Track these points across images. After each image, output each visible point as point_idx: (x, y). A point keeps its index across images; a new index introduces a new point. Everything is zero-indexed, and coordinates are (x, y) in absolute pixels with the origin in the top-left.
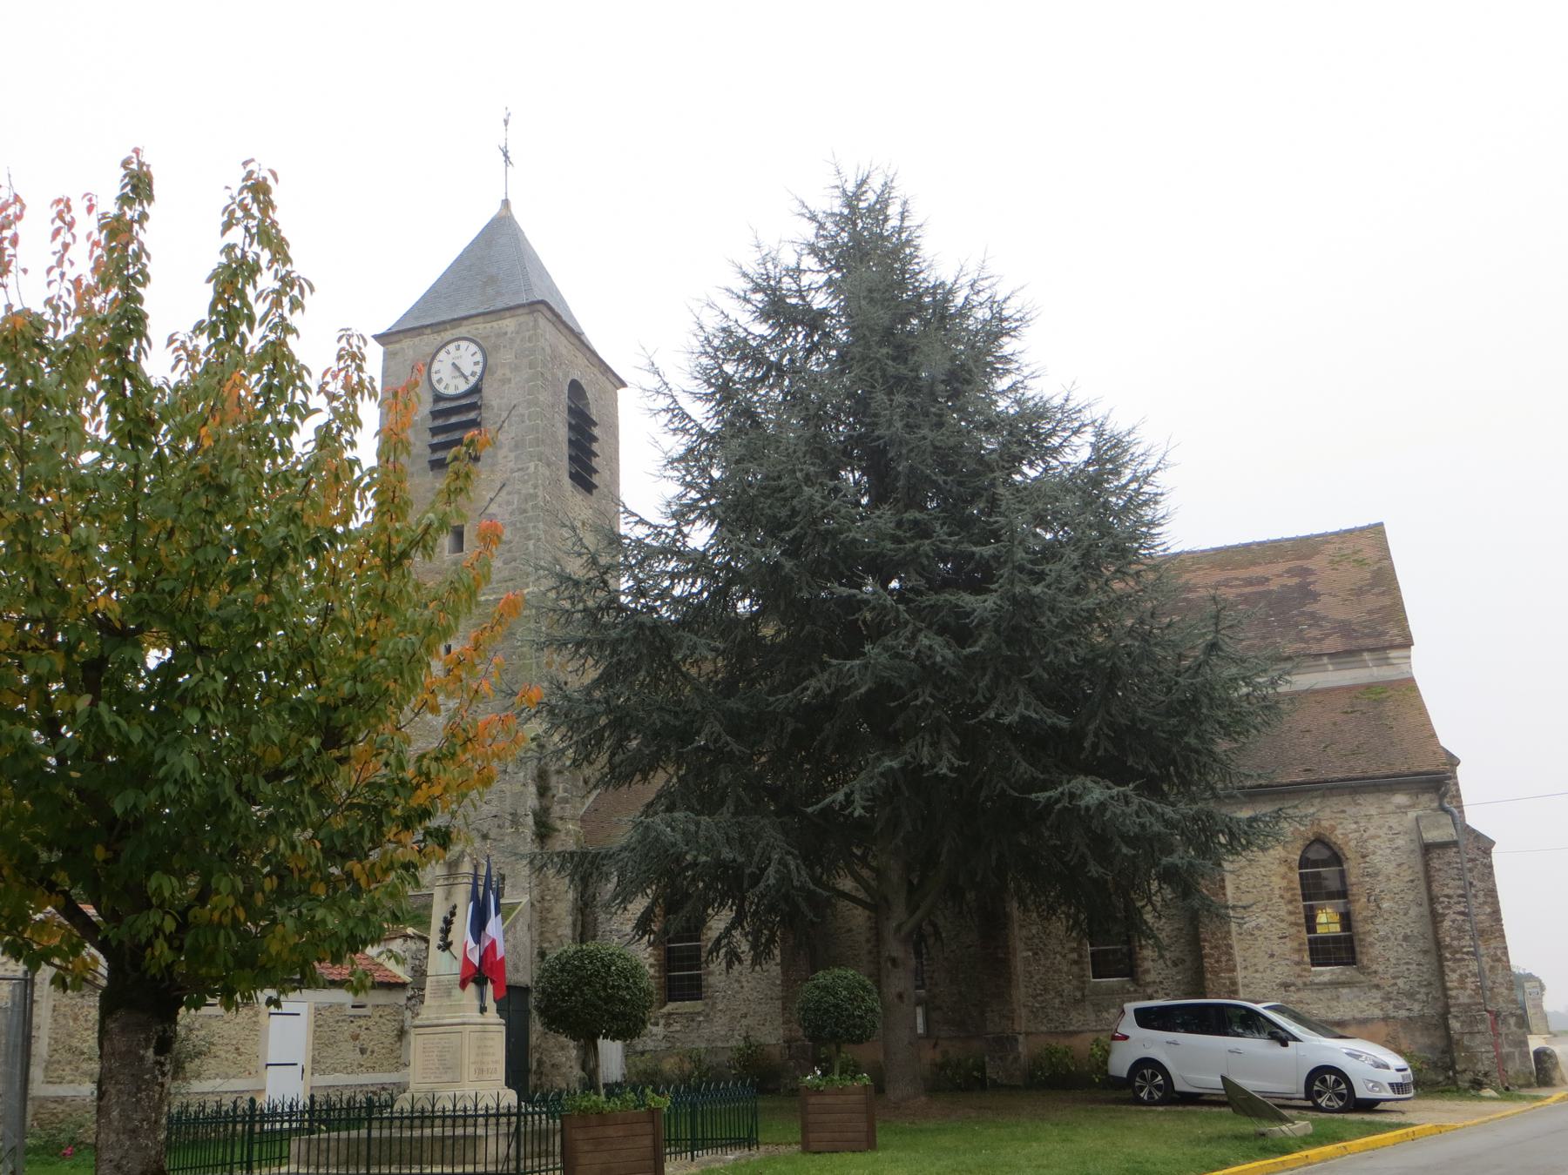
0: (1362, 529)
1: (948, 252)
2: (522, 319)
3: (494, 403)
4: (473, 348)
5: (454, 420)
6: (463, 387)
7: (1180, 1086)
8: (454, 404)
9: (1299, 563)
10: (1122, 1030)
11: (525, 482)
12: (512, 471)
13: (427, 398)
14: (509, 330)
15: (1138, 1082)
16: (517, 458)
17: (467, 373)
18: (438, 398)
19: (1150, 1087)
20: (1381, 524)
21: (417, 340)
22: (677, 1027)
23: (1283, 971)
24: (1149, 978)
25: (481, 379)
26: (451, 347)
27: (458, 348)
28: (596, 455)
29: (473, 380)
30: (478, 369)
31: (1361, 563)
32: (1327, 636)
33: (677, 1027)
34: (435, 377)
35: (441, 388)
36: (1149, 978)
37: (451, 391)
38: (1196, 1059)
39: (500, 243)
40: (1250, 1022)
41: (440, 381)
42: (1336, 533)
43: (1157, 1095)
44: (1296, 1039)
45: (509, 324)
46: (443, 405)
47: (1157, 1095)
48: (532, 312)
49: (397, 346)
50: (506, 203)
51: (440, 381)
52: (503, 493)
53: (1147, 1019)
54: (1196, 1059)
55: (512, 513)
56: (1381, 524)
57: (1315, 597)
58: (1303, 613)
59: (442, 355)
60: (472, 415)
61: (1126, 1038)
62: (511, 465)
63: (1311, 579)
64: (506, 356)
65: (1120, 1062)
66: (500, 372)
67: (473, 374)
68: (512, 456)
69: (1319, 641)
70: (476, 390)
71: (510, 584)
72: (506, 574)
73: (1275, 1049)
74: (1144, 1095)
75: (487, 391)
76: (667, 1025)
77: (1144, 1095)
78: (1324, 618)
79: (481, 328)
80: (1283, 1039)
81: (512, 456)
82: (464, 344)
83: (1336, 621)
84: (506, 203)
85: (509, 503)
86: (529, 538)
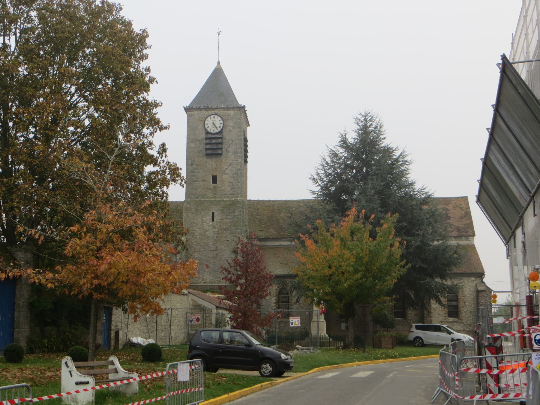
0: (462, 197)
1: (392, 139)
2: (236, 112)
3: (227, 138)
4: (219, 118)
5: (214, 141)
6: (216, 131)
7: (425, 343)
8: (214, 136)
9: (446, 206)
10: (412, 330)
11: (238, 165)
12: (233, 160)
13: (204, 132)
14: (232, 114)
15: (415, 342)
16: (235, 156)
17: (218, 126)
18: (207, 133)
19: (419, 343)
20: (467, 197)
21: (199, 112)
22: (282, 325)
23: (441, 318)
24: (409, 318)
25: (222, 129)
26: (212, 117)
27: (214, 118)
28: (156, 105)
29: (219, 129)
30: (221, 126)
31: (461, 208)
32: (453, 231)
33: (282, 325)
34: (206, 126)
35: (208, 130)
36: (409, 318)
37: (212, 131)
38: (429, 336)
39: (218, 75)
40: (437, 329)
41: (208, 127)
42: (454, 198)
43: (420, 345)
44: (452, 333)
45: (232, 113)
46: (209, 136)
47: (420, 345)
48: (239, 110)
49: (192, 113)
50: (219, 63)
51: (208, 127)
52: (230, 167)
53: (418, 328)
54: (429, 336)
55: (233, 174)
56: (467, 197)
57: (449, 218)
58: (447, 223)
59: (208, 119)
60: (220, 141)
61: (413, 332)
62: (233, 158)
63: (448, 212)
64: (231, 123)
65: (411, 337)
66: (228, 128)
67: (220, 127)
68: (233, 156)
69: (451, 232)
70: (221, 132)
71: (233, 196)
72: (231, 192)
73: (448, 335)
74: (417, 345)
75: (225, 133)
76: (279, 325)
77: (417, 345)
78: (452, 225)
79: (222, 112)
80: (450, 333)
81: (233, 156)
82: (216, 117)
83: (455, 226)
84: (219, 63)
85: (232, 171)
86: (239, 182)
